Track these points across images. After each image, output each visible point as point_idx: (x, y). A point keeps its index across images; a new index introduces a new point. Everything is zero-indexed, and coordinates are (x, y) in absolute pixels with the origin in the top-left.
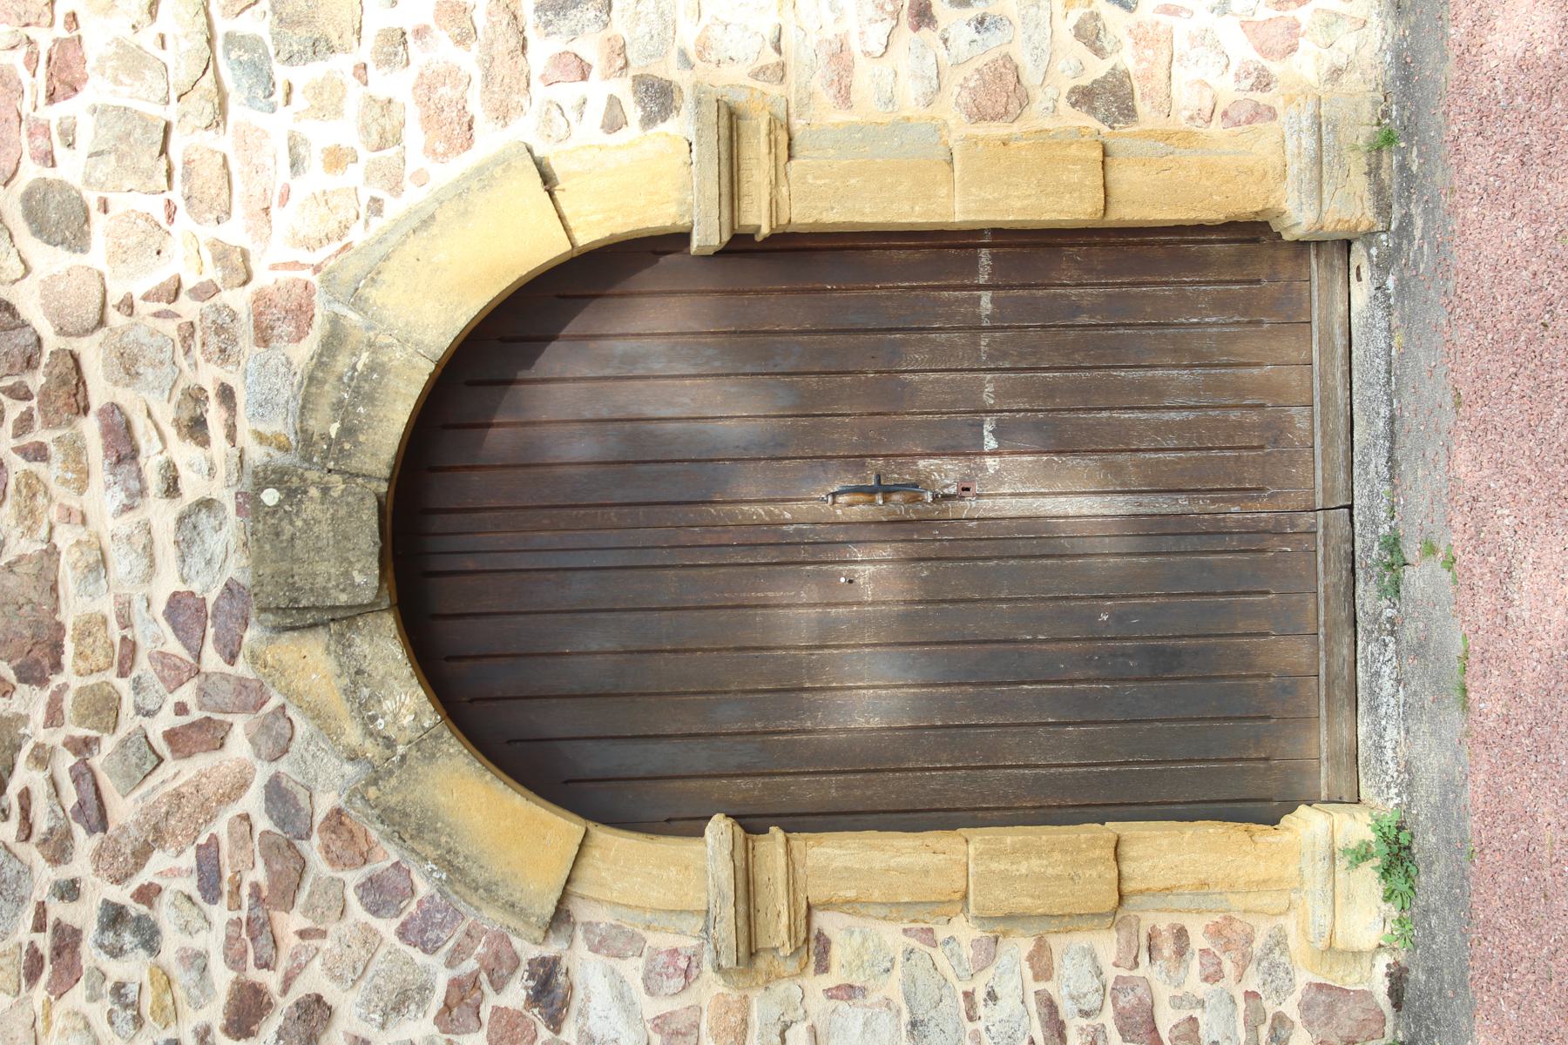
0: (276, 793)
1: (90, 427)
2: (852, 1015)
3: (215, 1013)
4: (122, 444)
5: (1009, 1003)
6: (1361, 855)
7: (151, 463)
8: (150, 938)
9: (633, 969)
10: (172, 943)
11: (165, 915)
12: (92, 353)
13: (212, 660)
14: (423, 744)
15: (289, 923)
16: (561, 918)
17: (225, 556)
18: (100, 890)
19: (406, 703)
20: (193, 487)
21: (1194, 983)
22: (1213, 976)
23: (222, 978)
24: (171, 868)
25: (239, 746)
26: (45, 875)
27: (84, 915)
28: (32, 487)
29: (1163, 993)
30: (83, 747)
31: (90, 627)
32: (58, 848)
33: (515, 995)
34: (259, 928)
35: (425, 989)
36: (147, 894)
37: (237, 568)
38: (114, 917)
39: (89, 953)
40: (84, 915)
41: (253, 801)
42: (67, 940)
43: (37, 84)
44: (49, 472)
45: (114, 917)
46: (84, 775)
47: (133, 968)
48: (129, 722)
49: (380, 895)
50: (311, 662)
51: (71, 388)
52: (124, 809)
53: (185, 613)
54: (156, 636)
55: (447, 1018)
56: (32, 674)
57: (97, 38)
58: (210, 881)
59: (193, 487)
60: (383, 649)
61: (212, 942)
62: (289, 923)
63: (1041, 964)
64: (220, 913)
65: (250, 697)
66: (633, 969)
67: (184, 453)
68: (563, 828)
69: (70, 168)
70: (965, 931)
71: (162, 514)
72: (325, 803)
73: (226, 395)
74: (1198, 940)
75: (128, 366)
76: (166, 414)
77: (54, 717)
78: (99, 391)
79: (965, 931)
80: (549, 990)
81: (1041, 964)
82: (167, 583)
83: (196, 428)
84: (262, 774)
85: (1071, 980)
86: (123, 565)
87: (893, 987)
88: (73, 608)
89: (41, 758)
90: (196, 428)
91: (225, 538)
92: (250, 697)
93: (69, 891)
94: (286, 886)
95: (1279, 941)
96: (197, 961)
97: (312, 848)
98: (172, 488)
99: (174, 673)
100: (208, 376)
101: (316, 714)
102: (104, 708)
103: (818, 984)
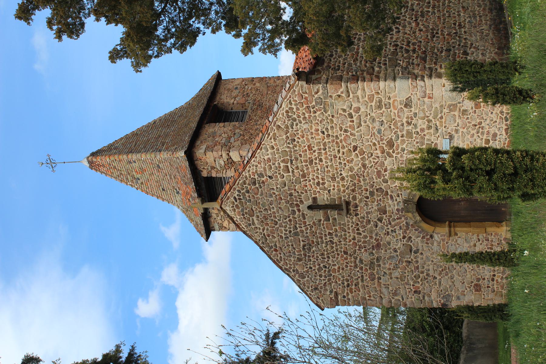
0: (406, 223)
1: (389, 196)
2: (460, 239)
3: (401, 237)
4: (392, 197)
5: (475, 238)
6: (509, 231)
7: (394, 199)
8: (395, 232)
9: (439, 235)
10: (397, 232)
11: (396, 230)
12: (389, 191)
13: (400, 213)
14: (420, 222)
15: (408, 232)
16: (433, 232)
17: (401, 206)
18: (391, 229)
19: (418, 218)
20: (398, 200)
21: (493, 237)
22: (495, 236)
23: (402, 235)
24: (397, 228)
25: (403, 219)
26: (386, 228)
27: (390, 230)
28: (384, 201)
29: (490, 238)
30: (389, 219)
31: (389, 211)
32: (387, 226)
33: (428, 237)
34: (405, 232)
35: (420, 236)
36: (395, 229)
37: (402, 206)
38: (392, 231)
39: (390, 233)
40: (390, 230)
41: (404, 223)
42: (388, 232)
43: (383, 172)
44: (385, 200)
45: (392, 231)
46: (389, 221)
47: (394, 234)
48: (393, 217)
49: (416, 230)
50: (410, 215)
51: (387, 194)
52: (393, 223)
53: (398, 210)
54: (395, 211)
55: (422, 238)
56: (384, 214)
57: (388, 168)
58: (401, 228)
59: (398, 200)
60: (417, 214)
61: (401, 232)
62: (408, 232)
63: (478, 236)
64: (402, 231)
65: (404, 216)
66: (439, 235)
67: (397, 198)
68: (433, 228)
69: (386, 177)
70: (471, 234)
71: (396, 203)
72: (411, 223)
73: (401, 194)
74: (493, 234)
75: (392, 192)
76: (396, 195)
77: (386, 216)
78: (389, 193)
79: (471, 234)
80: (432, 237)
81: (478, 236)
82: (396, 207)
83: (399, 196)
84: (405, 221)
85: (481, 237)
86: (392, 206)
87: (464, 237)
88: (388, 209)
89: (385, 220)
90: (399, 196)
91: (401, 204)
92: (404, 216)
93: (388, 229)
94: (408, 228)
95: (501, 234)
96: (400, 234)
97: (410, 227)
98: (396, 200)
99: (397, 214)
100: (400, 193)
101: (410, 218)
102: (391, 216)
103: (456, 237)
